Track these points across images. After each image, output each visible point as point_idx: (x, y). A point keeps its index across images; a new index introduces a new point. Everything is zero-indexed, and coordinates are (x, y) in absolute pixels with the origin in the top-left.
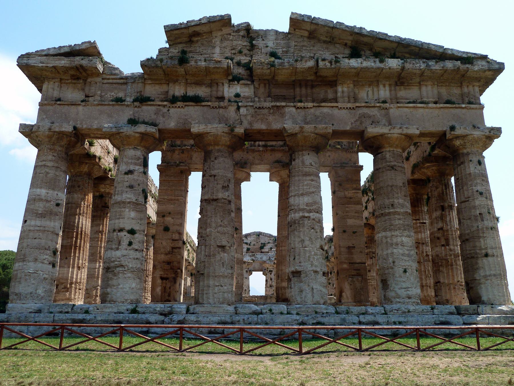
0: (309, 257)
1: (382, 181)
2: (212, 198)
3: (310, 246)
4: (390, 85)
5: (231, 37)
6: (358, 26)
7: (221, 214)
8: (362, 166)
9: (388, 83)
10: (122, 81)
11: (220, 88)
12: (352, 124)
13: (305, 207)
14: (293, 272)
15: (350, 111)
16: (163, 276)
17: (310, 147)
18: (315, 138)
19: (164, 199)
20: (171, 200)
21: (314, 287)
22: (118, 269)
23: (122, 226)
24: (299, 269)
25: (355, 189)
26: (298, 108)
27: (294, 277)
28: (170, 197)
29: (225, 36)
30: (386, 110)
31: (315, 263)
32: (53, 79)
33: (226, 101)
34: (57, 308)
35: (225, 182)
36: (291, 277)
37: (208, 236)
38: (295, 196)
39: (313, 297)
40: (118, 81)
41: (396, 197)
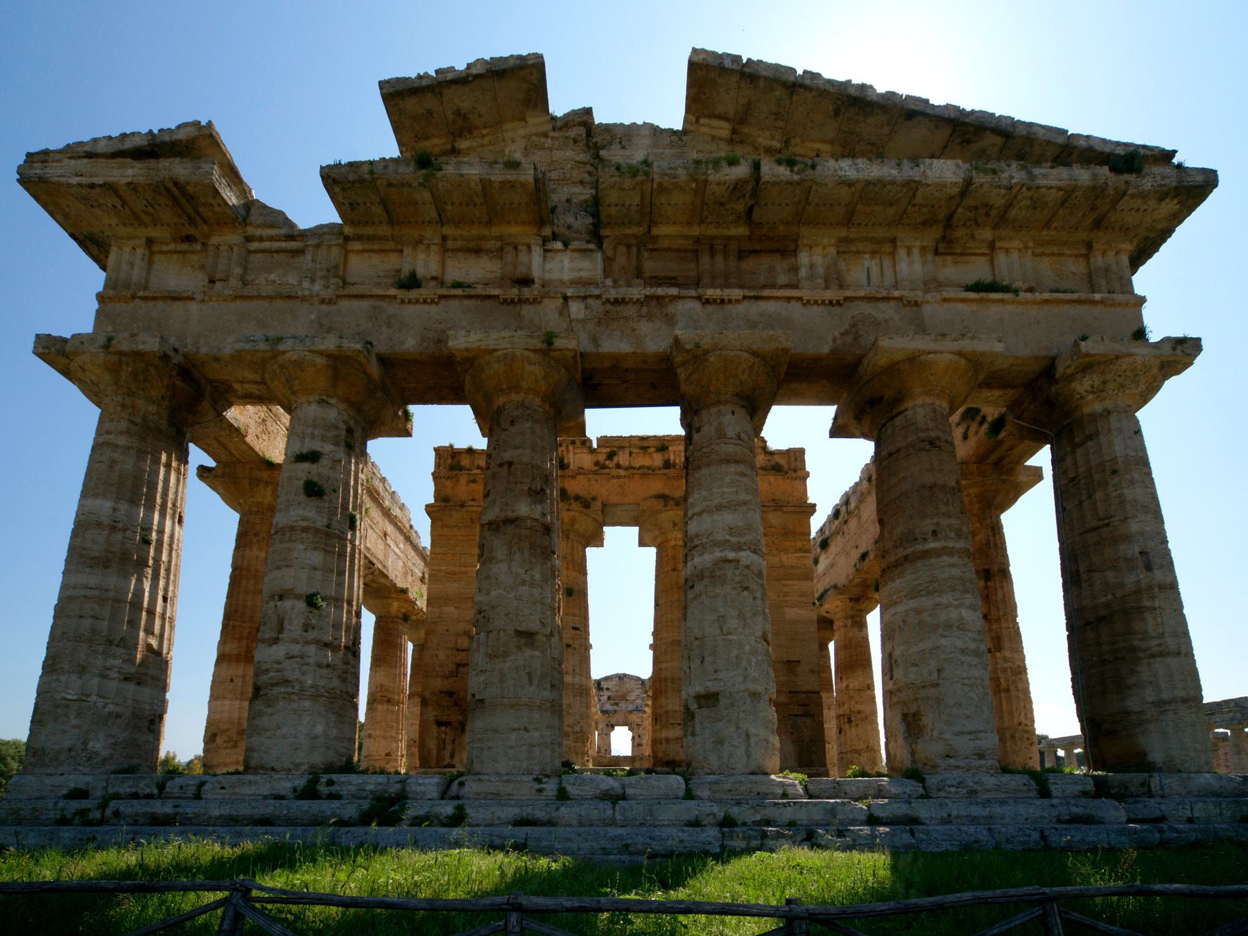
2: (502, 515)
4: (923, 249)
5: (549, 141)
6: (856, 81)
7: (527, 555)
9: (918, 243)
10: (292, 245)
11: (523, 257)
12: (834, 340)
13: (728, 537)
14: (698, 697)
15: (830, 308)
17: (737, 395)
21: (753, 730)
22: (276, 690)
23: (288, 584)
24: (713, 687)
26: (707, 301)
29: (534, 138)
30: (915, 309)
31: (753, 673)
32: (130, 238)
33: (537, 286)
34: (125, 785)
36: (694, 707)
37: (493, 608)
39: (749, 756)
40: (284, 245)
41: (944, 514)
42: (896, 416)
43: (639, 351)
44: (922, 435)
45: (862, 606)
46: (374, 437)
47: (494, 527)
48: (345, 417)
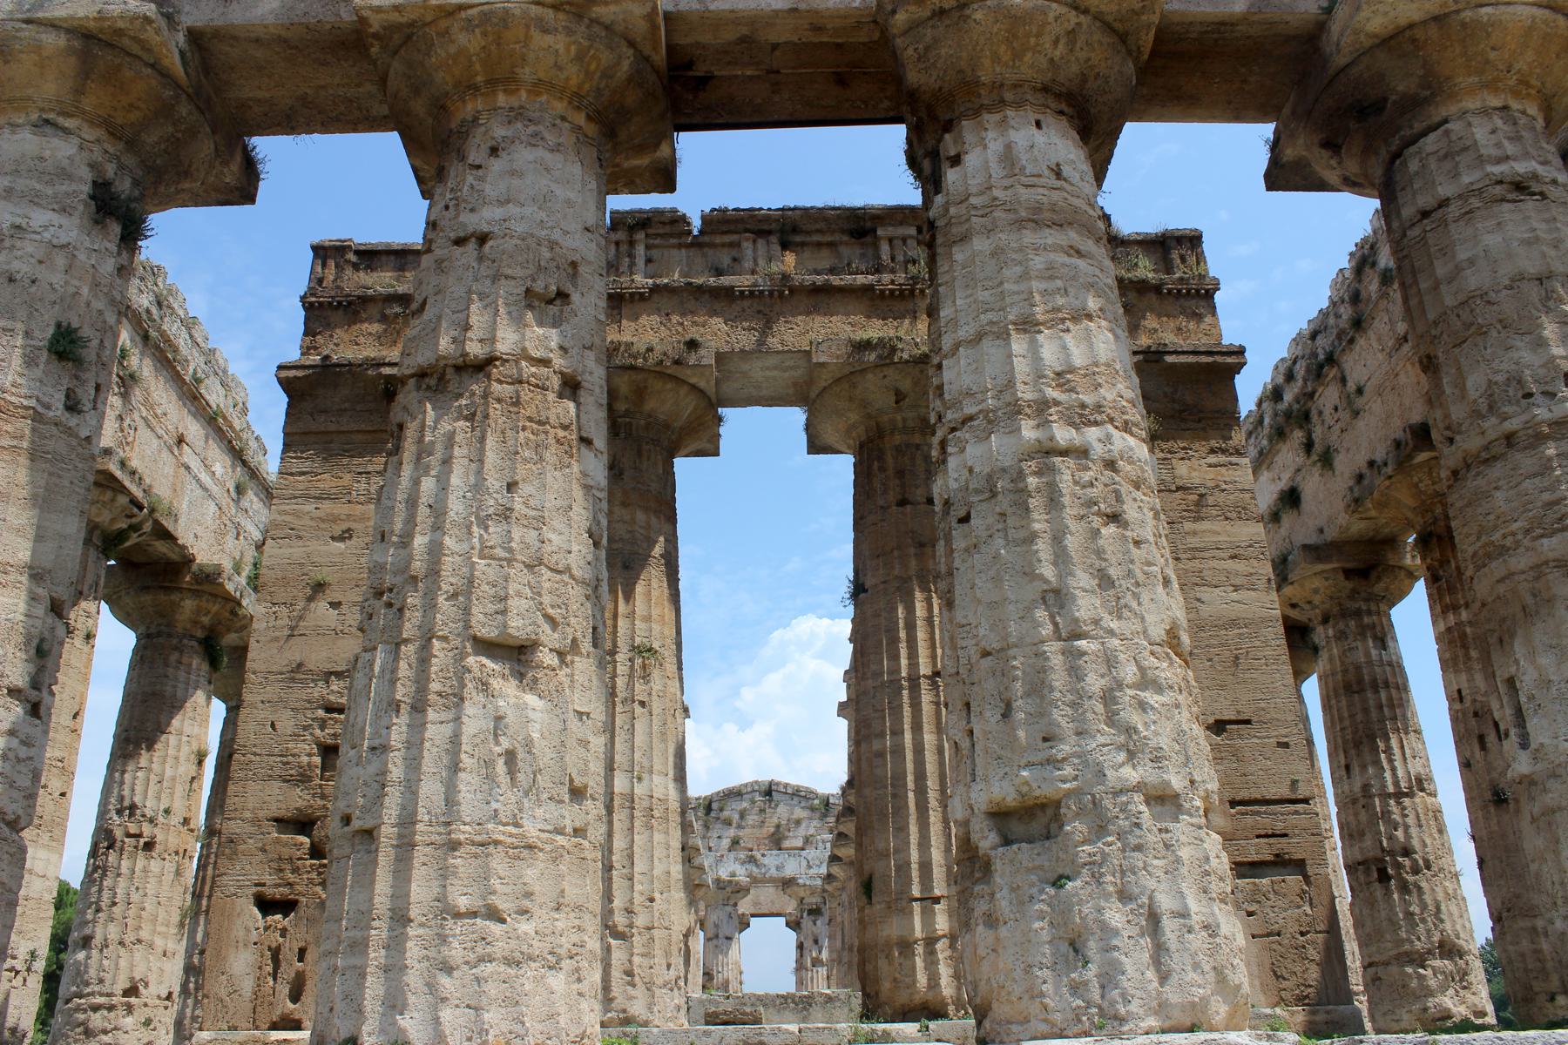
0: (1108, 698)
1: (1472, 262)
8: (1240, 351)
14: (1000, 816)
16: (269, 892)
17: (1045, 89)
18: (1072, 34)
27: (1007, 842)
36: (986, 840)
38: (978, 338)
42: (1424, 134)
43: (803, 6)
44: (1496, 170)
45: (1379, 588)
46: (164, 205)
47: (433, 382)
48: (97, 156)
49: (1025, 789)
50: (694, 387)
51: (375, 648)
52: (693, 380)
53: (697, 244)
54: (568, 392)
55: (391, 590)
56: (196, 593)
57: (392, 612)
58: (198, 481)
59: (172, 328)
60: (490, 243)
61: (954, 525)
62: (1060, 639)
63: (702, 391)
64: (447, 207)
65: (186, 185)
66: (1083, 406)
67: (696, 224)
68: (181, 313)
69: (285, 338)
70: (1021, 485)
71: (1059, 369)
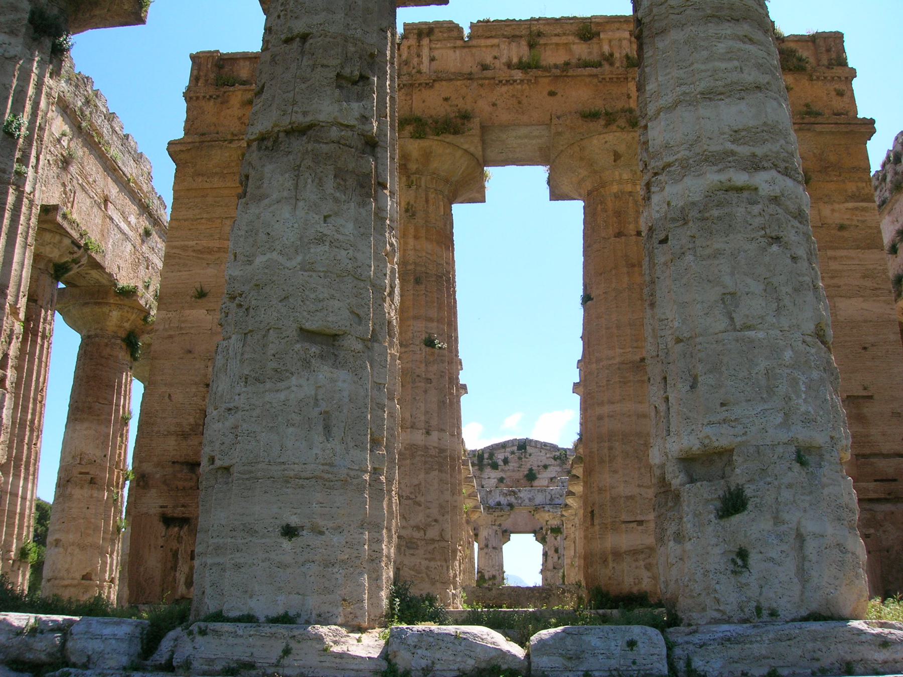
2: (285, 122)
3: (771, 319)
8: (872, 122)
13: (729, 146)
14: (687, 461)
16: (169, 512)
19: (185, 248)
20: (210, 251)
21: (810, 526)
24: (723, 438)
25: (853, 197)
27: (692, 481)
28: (204, 243)
31: (803, 405)
35: (347, 59)
36: (677, 479)
49: (706, 441)
50: (466, 151)
51: (230, 338)
52: (466, 146)
53: (466, 46)
54: (368, 149)
55: (241, 295)
56: (119, 307)
57: (241, 312)
58: (119, 228)
59: (99, 121)
60: (311, 41)
61: (656, 245)
62: (735, 330)
63: (472, 154)
64: (279, 17)
65: (97, 12)
66: (754, 155)
67: (467, 31)
68: (104, 110)
69: (173, 122)
70: (707, 215)
71: (736, 128)
